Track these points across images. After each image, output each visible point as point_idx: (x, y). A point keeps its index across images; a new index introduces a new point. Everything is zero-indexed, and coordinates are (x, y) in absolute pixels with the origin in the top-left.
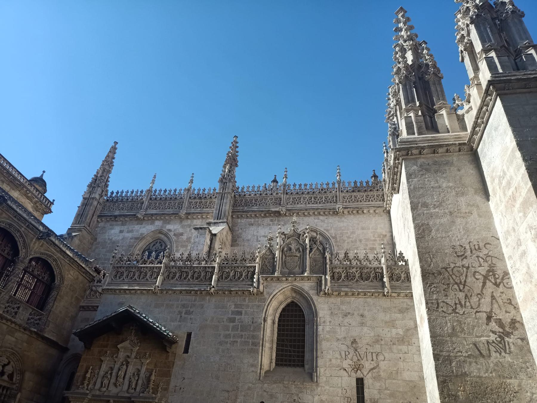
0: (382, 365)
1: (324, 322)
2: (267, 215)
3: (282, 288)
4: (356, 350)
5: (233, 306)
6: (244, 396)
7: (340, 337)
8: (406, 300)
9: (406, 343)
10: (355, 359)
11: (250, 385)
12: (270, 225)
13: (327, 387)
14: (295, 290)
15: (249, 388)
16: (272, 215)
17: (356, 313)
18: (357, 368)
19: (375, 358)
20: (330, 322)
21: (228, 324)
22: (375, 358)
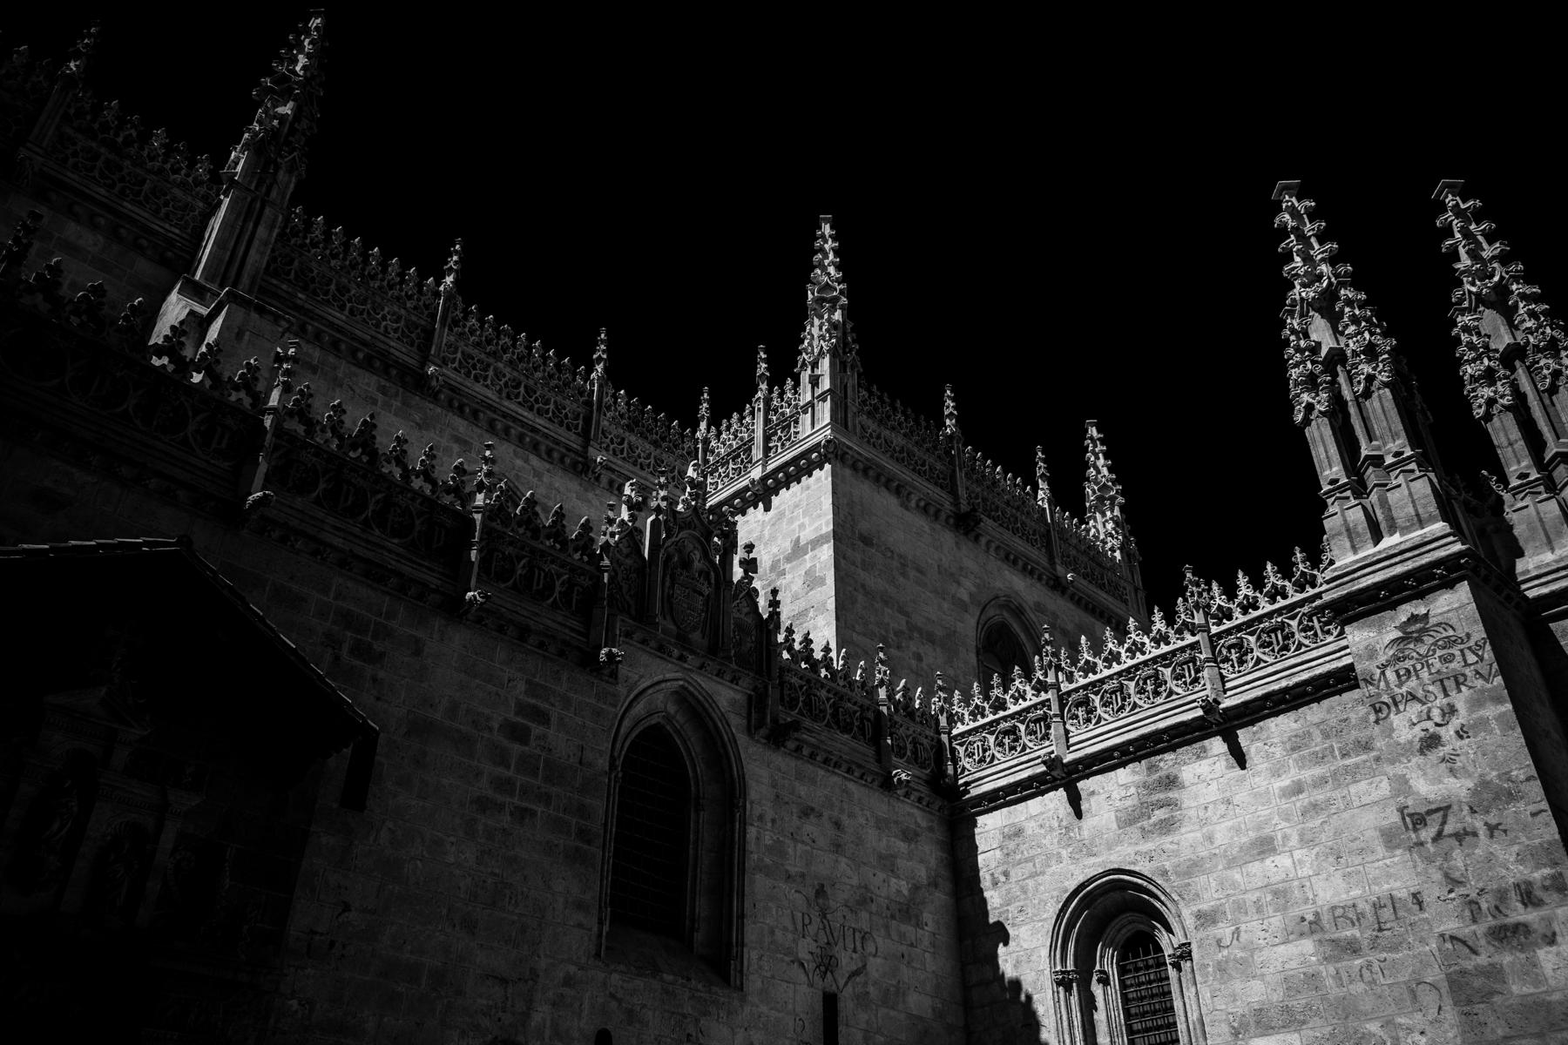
0: (875, 966)
1: (761, 818)
2: (377, 364)
3: (661, 677)
4: (824, 916)
5: (521, 686)
6: (554, 1004)
7: (793, 870)
8: (915, 811)
9: (913, 921)
10: (823, 940)
11: (572, 969)
12: (375, 402)
13: (764, 1009)
14: (684, 698)
15: (568, 981)
16: (394, 372)
17: (826, 814)
18: (827, 964)
19: (858, 944)
20: (773, 821)
21: (506, 743)
22: (858, 944)
